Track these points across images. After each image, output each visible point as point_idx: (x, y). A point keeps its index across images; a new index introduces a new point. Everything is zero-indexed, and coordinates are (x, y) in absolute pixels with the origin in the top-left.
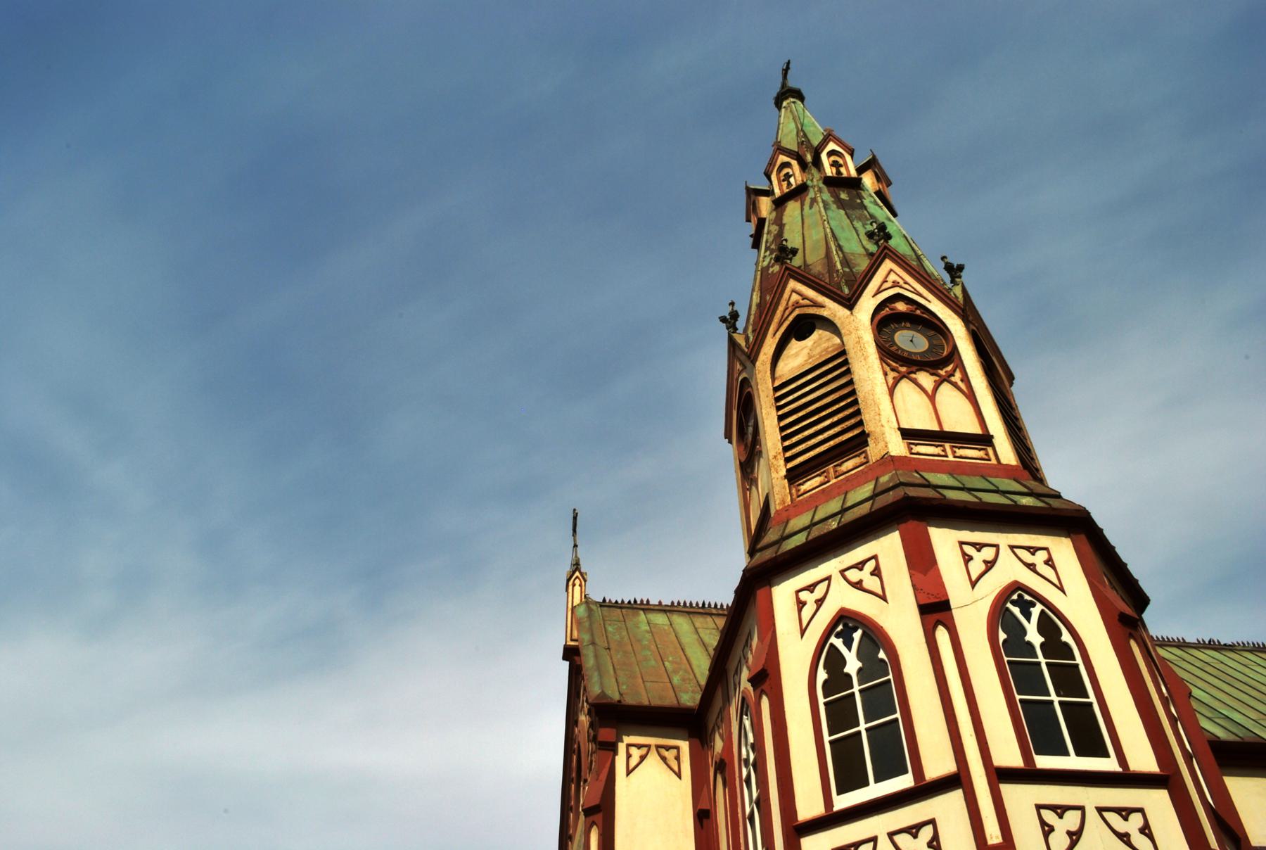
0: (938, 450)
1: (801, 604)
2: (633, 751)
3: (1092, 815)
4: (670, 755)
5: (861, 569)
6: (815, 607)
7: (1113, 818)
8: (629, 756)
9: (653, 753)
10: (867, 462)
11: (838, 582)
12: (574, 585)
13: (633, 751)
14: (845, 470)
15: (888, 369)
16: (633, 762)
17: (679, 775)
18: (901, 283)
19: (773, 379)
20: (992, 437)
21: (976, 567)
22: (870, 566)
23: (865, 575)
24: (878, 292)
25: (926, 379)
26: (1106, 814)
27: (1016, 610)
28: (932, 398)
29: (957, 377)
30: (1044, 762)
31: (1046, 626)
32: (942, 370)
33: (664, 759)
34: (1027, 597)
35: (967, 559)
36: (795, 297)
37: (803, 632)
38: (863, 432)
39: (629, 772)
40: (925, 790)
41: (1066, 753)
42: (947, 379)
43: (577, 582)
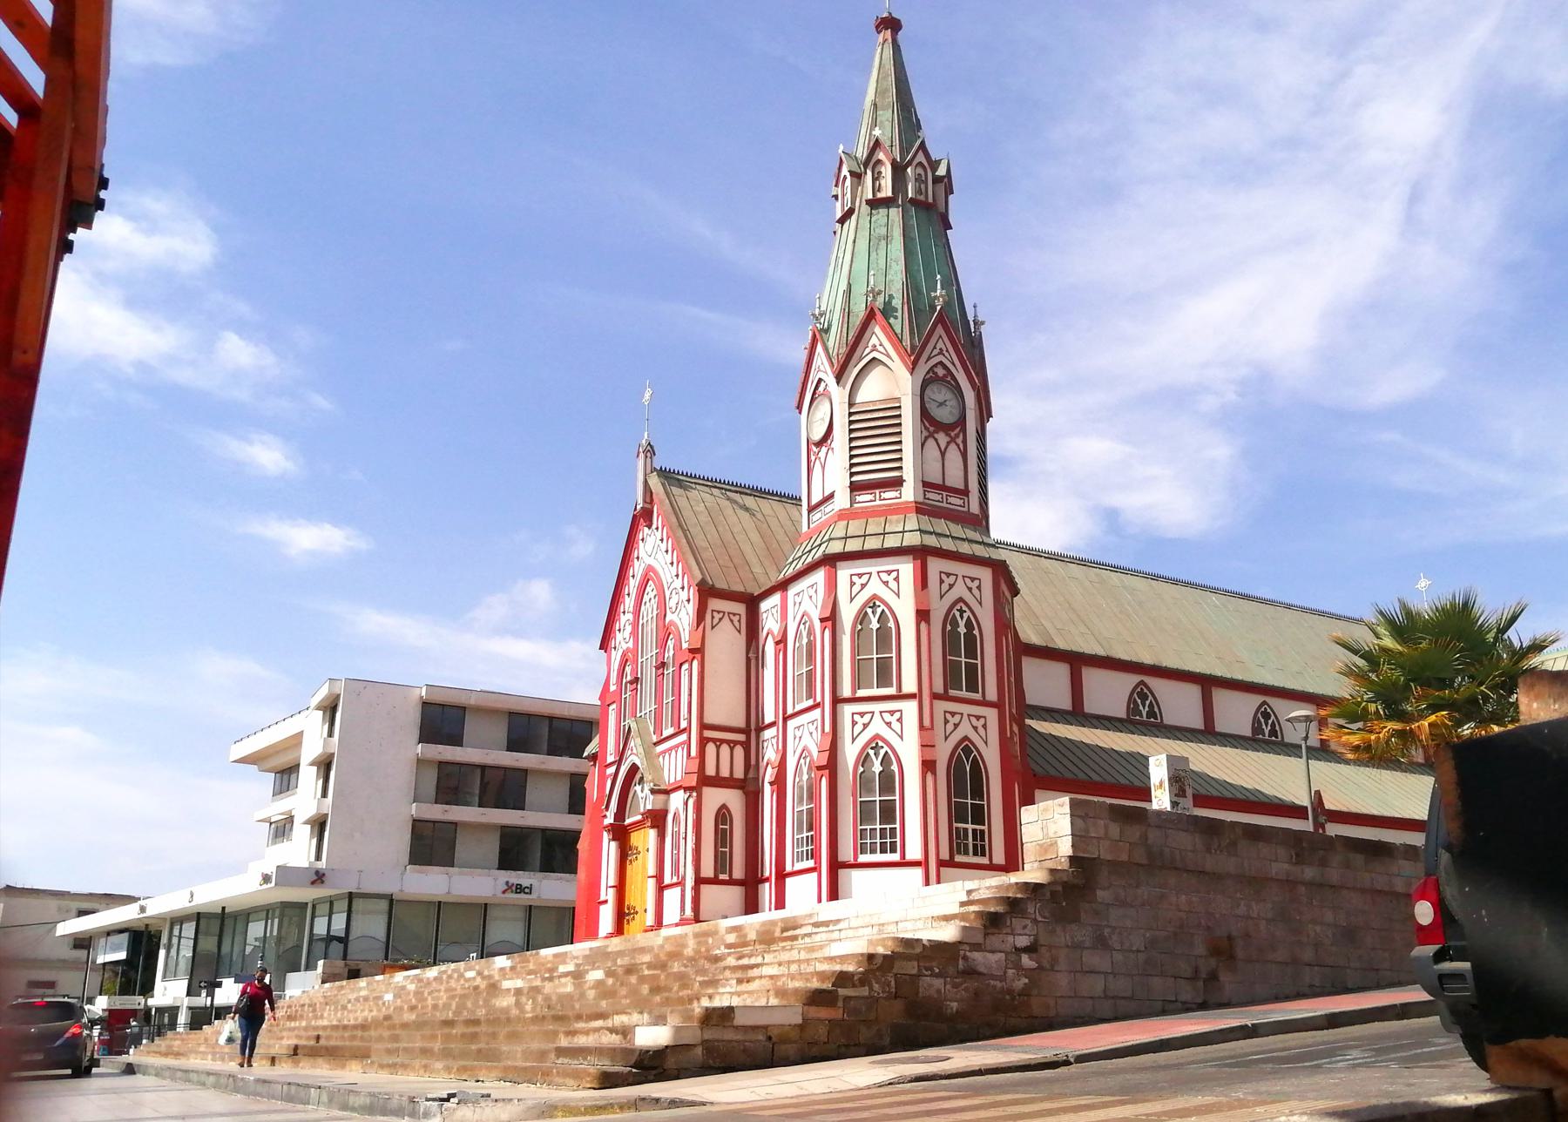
0: (939, 497)
1: (852, 584)
2: (715, 614)
3: (965, 717)
4: (736, 619)
8: (713, 617)
9: (726, 618)
13: (715, 614)
15: (923, 428)
17: (739, 632)
18: (944, 352)
19: (851, 405)
23: (890, 578)
24: (929, 358)
25: (942, 438)
26: (971, 718)
27: (958, 614)
28: (943, 454)
29: (959, 441)
30: (953, 693)
31: (969, 625)
32: (953, 431)
33: (732, 621)
34: (964, 608)
37: (852, 600)
38: (901, 476)
39: (713, 628)
41: (962, 690)
42: (953, 440)
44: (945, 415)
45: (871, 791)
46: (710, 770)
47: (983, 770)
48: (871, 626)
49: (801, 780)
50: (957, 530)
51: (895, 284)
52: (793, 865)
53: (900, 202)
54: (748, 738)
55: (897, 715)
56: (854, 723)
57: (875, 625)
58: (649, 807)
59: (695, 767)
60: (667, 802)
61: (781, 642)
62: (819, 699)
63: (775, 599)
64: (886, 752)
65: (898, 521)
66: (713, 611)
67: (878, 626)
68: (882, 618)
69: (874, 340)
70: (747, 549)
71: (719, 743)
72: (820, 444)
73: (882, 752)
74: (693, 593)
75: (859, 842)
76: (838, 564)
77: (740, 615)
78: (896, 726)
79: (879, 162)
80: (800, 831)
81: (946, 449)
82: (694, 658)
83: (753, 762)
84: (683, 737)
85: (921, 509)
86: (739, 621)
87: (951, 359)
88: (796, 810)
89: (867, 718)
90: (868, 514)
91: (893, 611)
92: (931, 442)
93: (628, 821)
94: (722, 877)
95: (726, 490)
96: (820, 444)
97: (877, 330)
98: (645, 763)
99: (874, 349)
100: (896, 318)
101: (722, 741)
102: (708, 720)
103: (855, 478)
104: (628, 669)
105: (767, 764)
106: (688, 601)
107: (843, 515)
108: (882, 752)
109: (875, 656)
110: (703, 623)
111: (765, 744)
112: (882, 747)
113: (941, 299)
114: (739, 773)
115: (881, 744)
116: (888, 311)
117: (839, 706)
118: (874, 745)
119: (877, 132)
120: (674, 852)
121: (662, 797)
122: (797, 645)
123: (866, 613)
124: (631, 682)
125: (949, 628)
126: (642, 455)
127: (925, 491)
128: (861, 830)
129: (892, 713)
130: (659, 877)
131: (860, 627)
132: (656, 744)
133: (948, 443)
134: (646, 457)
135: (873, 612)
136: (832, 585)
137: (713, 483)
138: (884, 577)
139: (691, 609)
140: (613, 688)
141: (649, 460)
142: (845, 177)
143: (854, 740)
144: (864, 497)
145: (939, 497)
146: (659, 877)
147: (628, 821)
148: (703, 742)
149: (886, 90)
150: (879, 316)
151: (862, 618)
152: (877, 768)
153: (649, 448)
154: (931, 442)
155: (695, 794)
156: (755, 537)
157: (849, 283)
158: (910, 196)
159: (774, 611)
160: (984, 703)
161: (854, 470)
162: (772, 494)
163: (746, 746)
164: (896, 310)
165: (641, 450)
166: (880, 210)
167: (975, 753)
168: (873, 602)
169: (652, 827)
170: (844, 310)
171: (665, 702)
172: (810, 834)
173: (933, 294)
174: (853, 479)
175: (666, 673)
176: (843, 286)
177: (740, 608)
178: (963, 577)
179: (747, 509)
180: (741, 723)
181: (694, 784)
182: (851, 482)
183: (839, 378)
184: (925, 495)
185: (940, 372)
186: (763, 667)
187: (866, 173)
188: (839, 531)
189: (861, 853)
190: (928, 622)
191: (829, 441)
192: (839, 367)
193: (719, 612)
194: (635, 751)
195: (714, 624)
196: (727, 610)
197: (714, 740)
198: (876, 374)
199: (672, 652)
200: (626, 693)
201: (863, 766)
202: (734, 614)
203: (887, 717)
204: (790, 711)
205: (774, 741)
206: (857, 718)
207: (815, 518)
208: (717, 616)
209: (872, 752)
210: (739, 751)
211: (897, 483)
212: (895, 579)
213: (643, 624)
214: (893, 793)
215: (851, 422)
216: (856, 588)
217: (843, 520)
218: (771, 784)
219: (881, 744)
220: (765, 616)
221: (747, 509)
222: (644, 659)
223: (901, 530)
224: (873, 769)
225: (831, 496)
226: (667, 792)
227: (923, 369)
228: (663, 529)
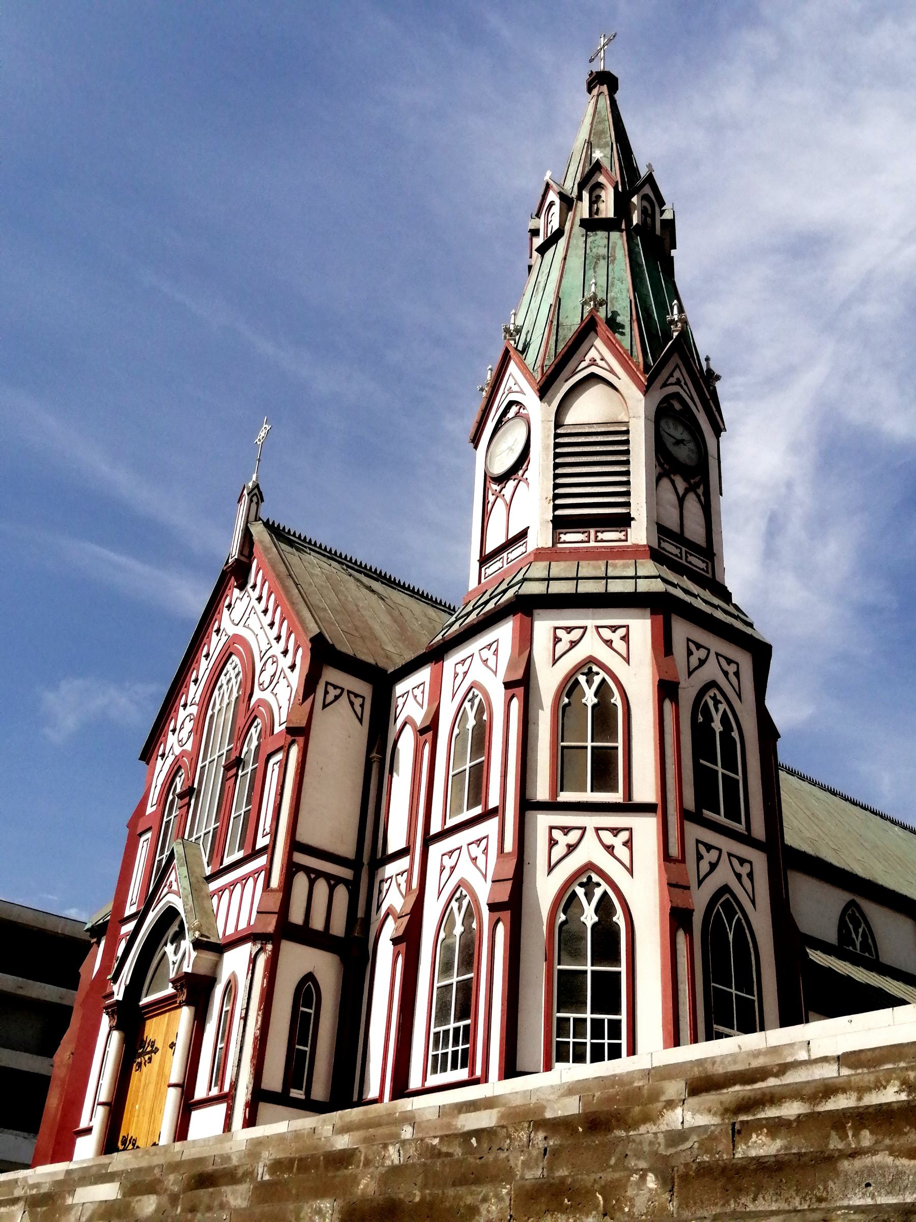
0: (677, 552)
1: (557, 640)
2: (330, 688)
3: (725, 856)
4: (357, 702)
5: (614, 632)
6: (568, 645)
7: (735, 862)
8: (326, 692)
10: (626, 540)
11: (591, 633)
13: (330, 688)
16: (330, 698)
17: (361, 720)
18: (683, 383)
19: (558, 425)
20: (715, 554)
21: (694, 661)
22: (622, 632)
23: (616, 637)
24: (665, 385)
27: (711, 703)
28: (681, 501)
29: (700, 491)
33: (352, 704)
34: (719, 697)
35: (690, 653)
37: (555, 662)
38: (629, 514)
39: (325, 706)
40: (629, 807)
44: (684, 453)
45: (577, 955)
46: (296, 916)
47: (751, 945)
48: (584, 701)
49: (450, 934)
50: (707, 595)
51: (621, 302)
52: (425, 1078)
53: (623, 227)
54: (357, 876)
55: (624, 836)
56: (553, 843)
57: (590, 699)
58: (187, 968)
59: (274, 903)
60: (217, 965)
61: (430, 728)
62: (493, 802)
63: (424, 675)
64: (605, 893)
65: (625, 566)
66: (327, 683)
67: (595, 701)
68: (602, 691)
69: (593, 353)
70: (377, 628)
71: (314, 875)
72: (502, 479)
73: (598, 892)
74: (302, 658)
75: (555, 1039)
76: (537, 612)
77: (364, 698)
78: (622, 852)
79: (600, 186)
80: (442, 1018)
81: (685, 495)
82: (293, 742)
83: (360, 914)
84: (262, 861)
85: (656, 555)
86: (362, 706)
87: (688, 393)
88: (436, 985)
89: (574, 836)
90: (578, 555)
91: (620, 683)
92: (665, 482)
93: (144, 1001)
94: (296, 1093)
95: (348, 566)
96: (502, 479)
97: (598, 343)
98: (191, 903)
99: (593, 362)
100: (623, 334)
101: (320, 874)
102: (303, 836)
103: (559, 512)
104: (179, 781)
105: (387, 915)
106: (292, 667)
107: (540, 554)
108: (598, 892)
109: (589, 744)
110: (312, 696)
111: (386, 886)
112: (598, 885)
113: (679, 325)
114: (338, 928)
115: (596, 878)
116: (613, 324)
117: (529, 814)
118: (585, 880)
119: (597, 155)
120: (219, 1046)
121: (209, 956)
122: (456, 731)
123: (577, 682)
124: (181, 796)
125: (701, 719)
126: (246, 498)
127: (659, 539)
128: (559, 1019)
129: (616, 831)
130: (187, 1086)
131: (566, 700)
132: (210, 879)
133: (687, 491)
134: (251, 501)
135: (587, 681)
136: (525, 640)
137: (332, 556)
138: (607, 634)
139: (296, 679)
140: (150, 810)
141: (254, 506)
142: (552, 204)
143: (551, 869)
144: (572, 538)
145: (677, 552)
146: (187, 1086)
147: (144, 1001)
148: (291, 870)
149: (603, 132)
150: (602, 327)
151: (570, 687)
152: (589, 917)
153: (256, 491)
154: (665, 482)
155: (269, 947)
156: (387, 620)
157: (558, 296)
158: (635, 222)
159: (418, 692)
160: (747, 839)
161: (558, 502)
162: (403, 587)
163: (353, 887)
164: (623, 327)
165: (245, 492)
166: (598, 232)
167: (739, 914)
168: (588, 666)
169: (188, 1003)
170: (552, 322)
171: (233, 816)
172: (461, 1024)
173: (669, 318)
174: (557, 513)
175: (240, 773)
176: (550, 299)
177: (364, 688)
178: (717, 655)
179: (373, 591)
180: (347, 849)
181: (271, 929)
182: (554, 516)
183: (543, 392)
184: (659, 543)
185: (678, 406)
186: (391, 773)
187: (580, 198)
188: (540, 569)
189: (557, 1061)
190: (675, 700)
191: (520, 472)
192: (544, 378)
193: (335, 687)
194: (175, 887)
195: (327, 702)
196: (346, 688)
197: (308, 870)
198: (596, 392)
199: (255, 743)
200: (170, 814)
201: (565, 912)
202: (356, 696)
203: (607, 837)
204: (436, 827)
205: (402, 880)
206: (557, 834)
207: (489, 571)
208: (333, 693)
209: (580, 892)
210: (342, 893)
211: (623, 522)
212: (623, 638)
213: (212, 716)
214: (616, 961)
215: (556, 446)
216: (561, 647)
217: (541, 560)
218: (395, 941)
219: (596, 878)
220: (400, 701)
221: (373, 591)
222: (207, 762)
223: (632, 574)
224: (582, 919)
225: (523, 534)
226: (220, 949)
227: (658, 395)
228: (263, 585)
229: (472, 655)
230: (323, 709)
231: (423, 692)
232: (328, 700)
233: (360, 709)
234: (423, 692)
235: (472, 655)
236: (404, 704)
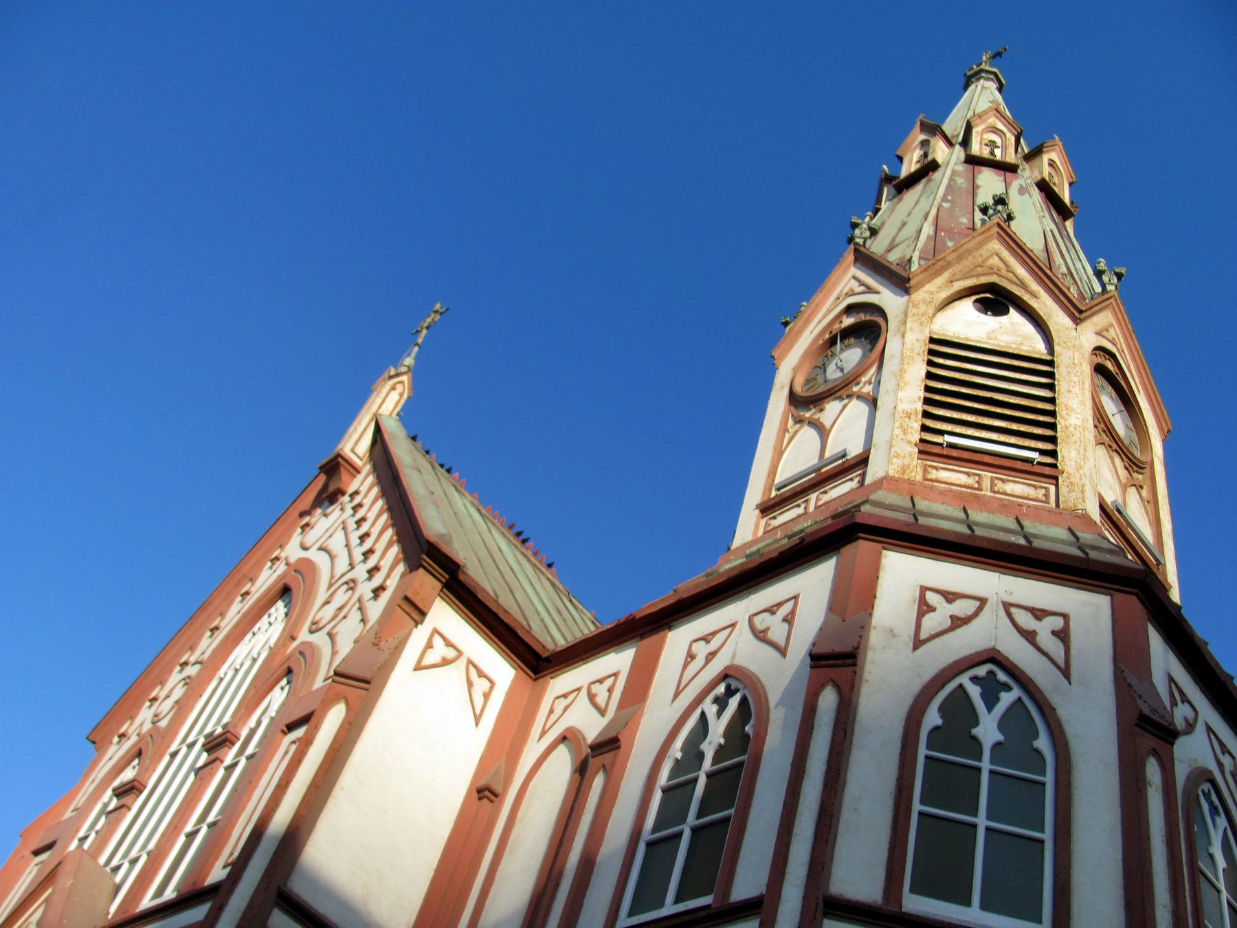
2: (437, 641)
4: (481, 685)
8: (429, 645)
12: (393, 388)
13: (437, 641)
14: (1009, 491)
16: (432, 657)
17: (477, 720)
33: (470, 684)
36: (995, 261)
43: (399, 388)
66: (436, 631)
193: (449, 644)
202: (481, 674)
229: (733, 625)
230: (415, 669)
231: (610, 690)
232: (428, 660)
233: (482, 698)
234: (610, 690)
235: (733, 625)
236: (567, 708)
